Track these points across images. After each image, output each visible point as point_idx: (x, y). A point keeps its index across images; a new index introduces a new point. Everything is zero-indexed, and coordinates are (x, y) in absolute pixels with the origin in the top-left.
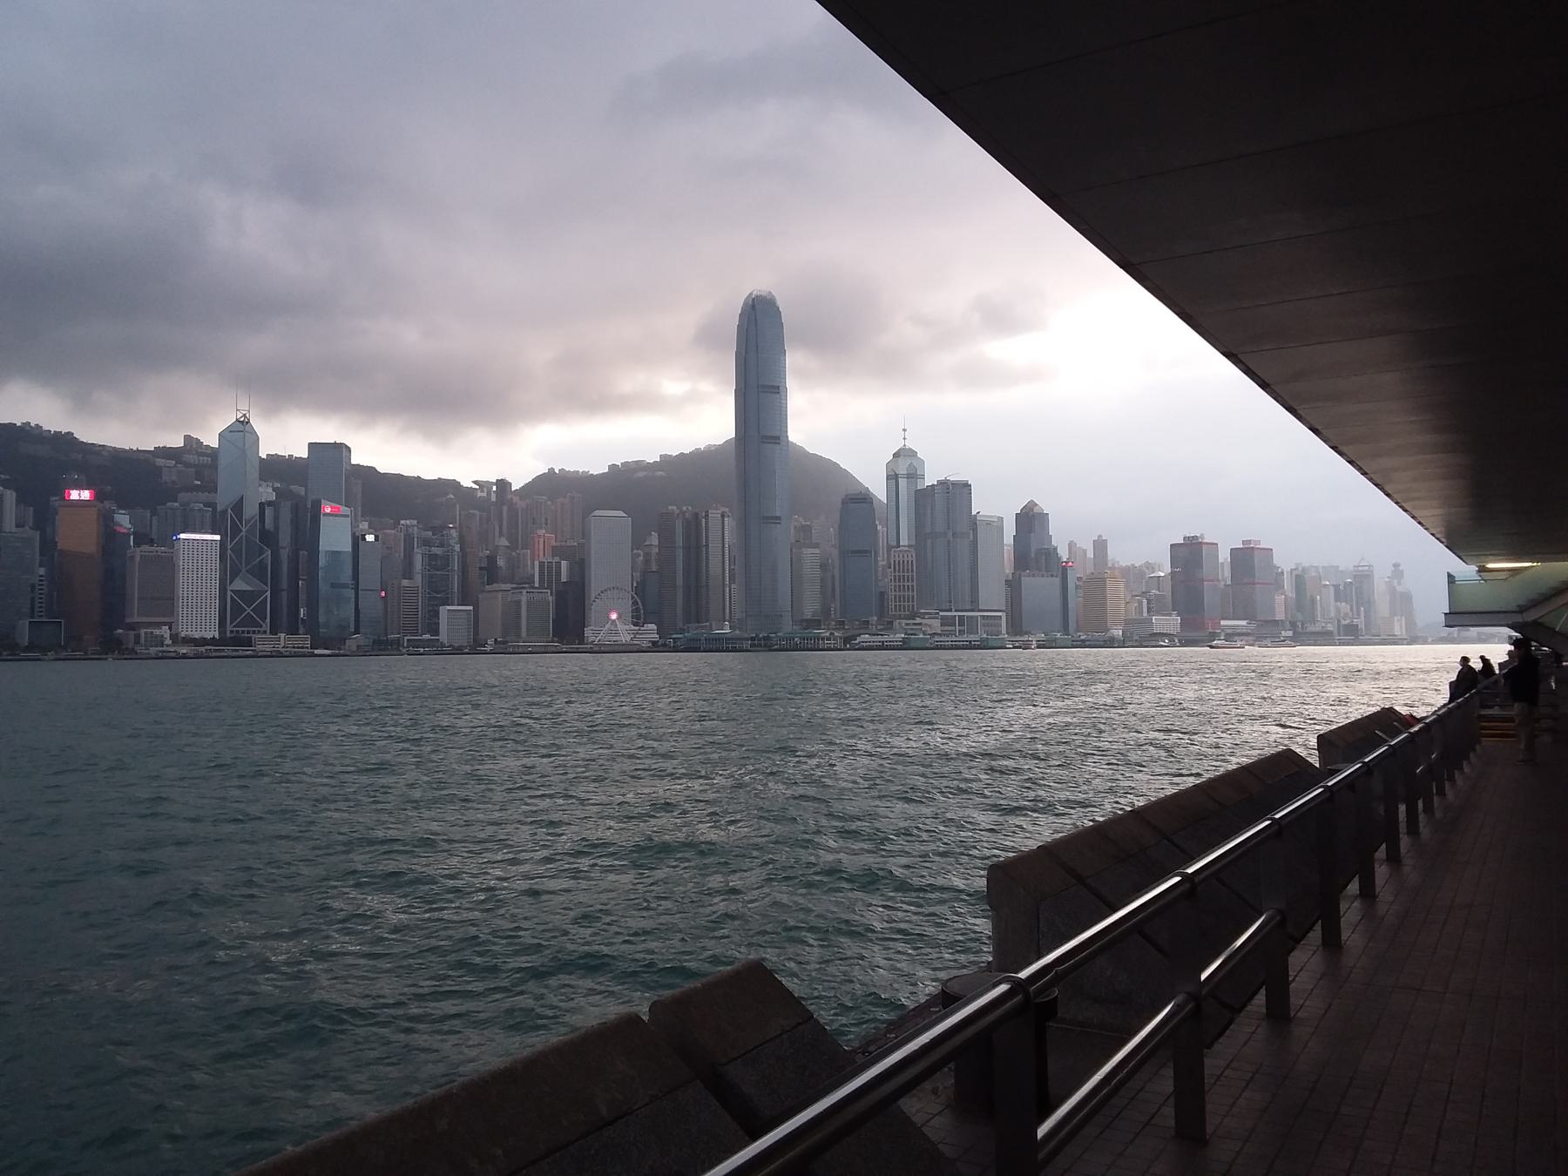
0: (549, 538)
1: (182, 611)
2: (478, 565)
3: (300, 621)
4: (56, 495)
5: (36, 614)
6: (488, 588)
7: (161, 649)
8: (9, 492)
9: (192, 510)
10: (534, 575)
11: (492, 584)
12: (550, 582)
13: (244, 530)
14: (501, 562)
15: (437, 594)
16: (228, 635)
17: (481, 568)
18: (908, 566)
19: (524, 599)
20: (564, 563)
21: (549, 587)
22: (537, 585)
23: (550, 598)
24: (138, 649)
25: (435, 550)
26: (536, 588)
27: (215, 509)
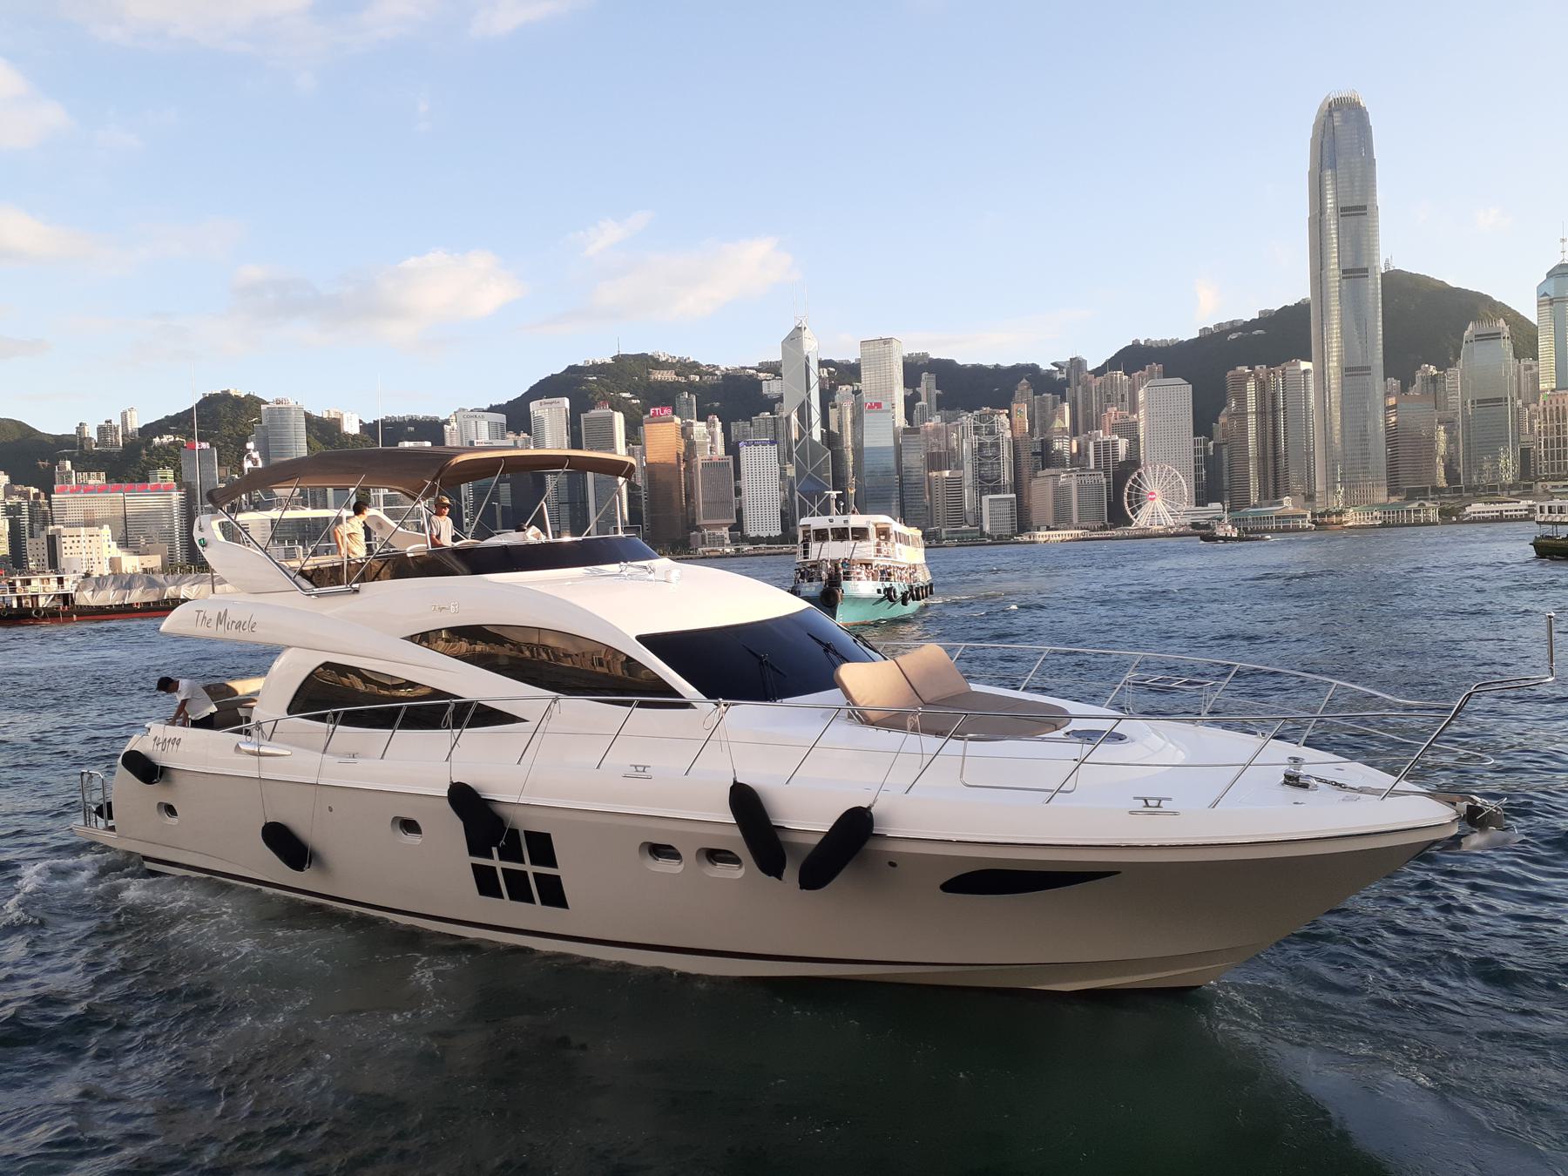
6: (1040, 473)
13: (807, 433)
15: (987, 484)
17: (1034, 454)
18: (1558, 413)
19: (1074, 483)
20: (1123, 445)
23: (1104, 481)
25: (989, 440)
26: (1091, 470)
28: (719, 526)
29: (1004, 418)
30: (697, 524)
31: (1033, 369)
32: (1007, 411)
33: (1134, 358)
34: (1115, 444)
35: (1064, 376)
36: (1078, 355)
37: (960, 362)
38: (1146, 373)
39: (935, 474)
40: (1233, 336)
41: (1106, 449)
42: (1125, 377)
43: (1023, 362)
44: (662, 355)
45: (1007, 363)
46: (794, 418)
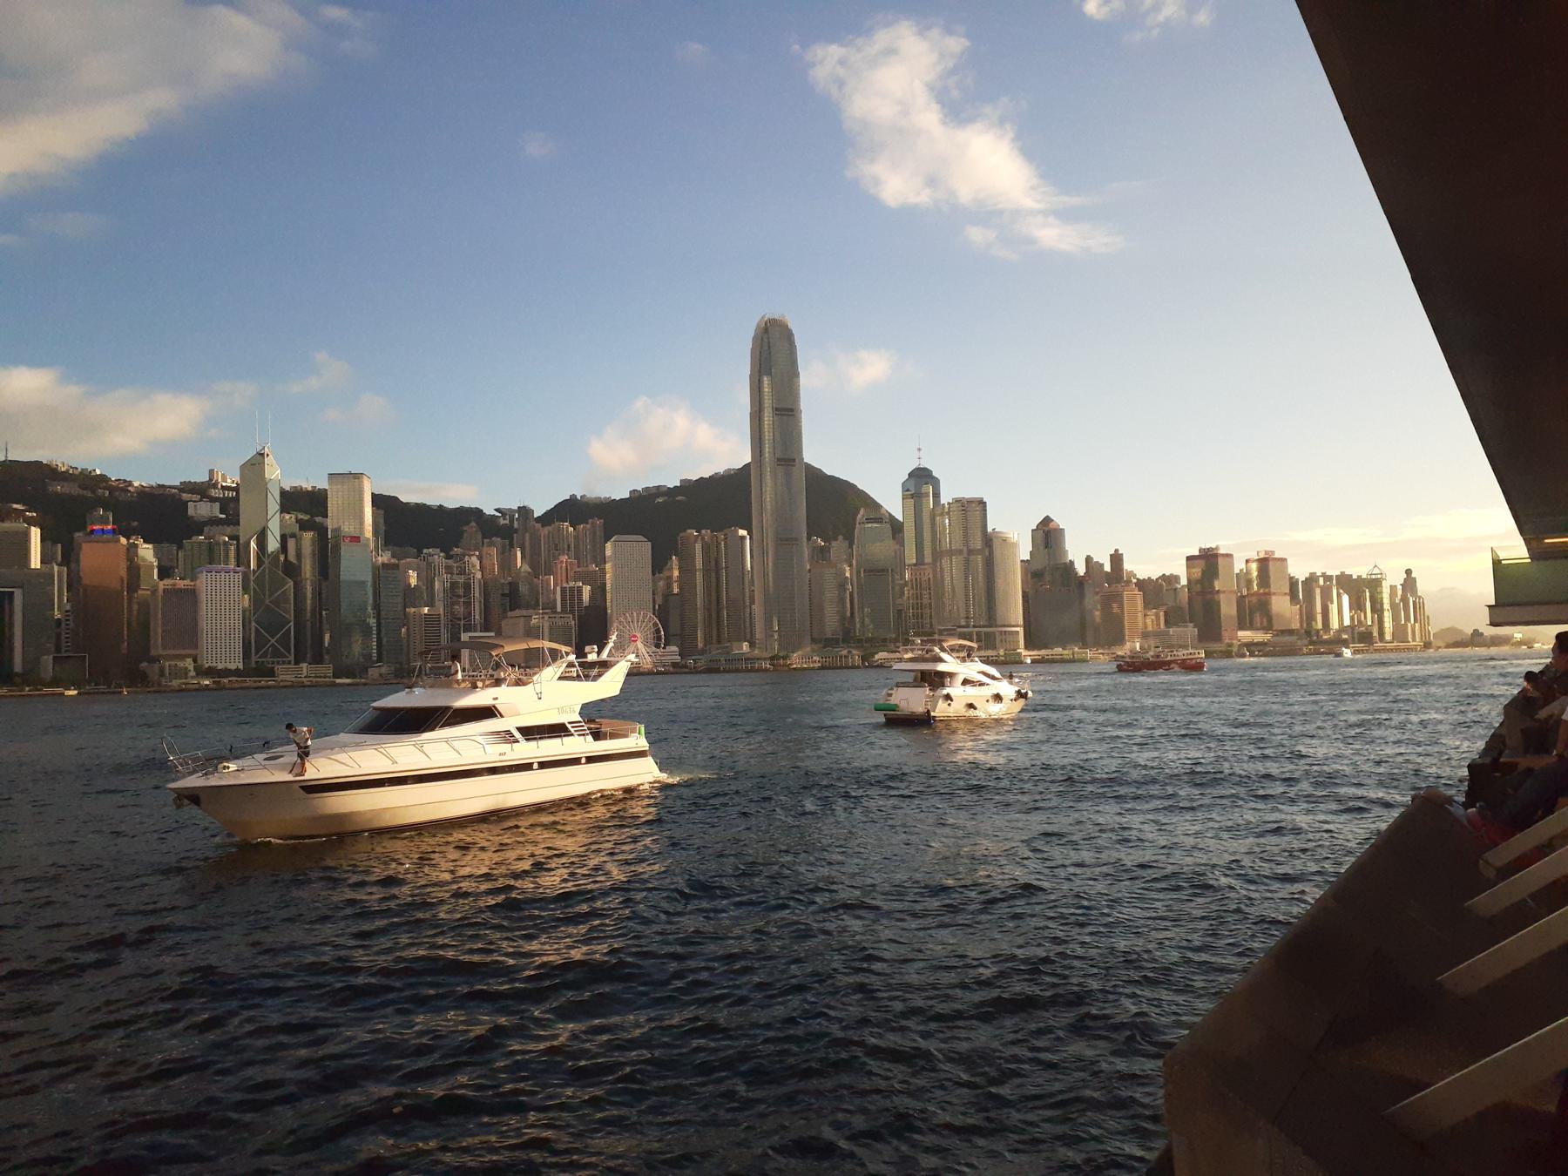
0: (572, 564)
1: (204, 642)
2: (500, 592)
3: (324, 651)
4: (79, 531)
5: (63, 650)
6: (510, 614)
7: (184, 681)
8: (33, 528)
9: (219, 544)
10: (555, 600)
11: (514, 610)
12: (572, 606)
14: (523, 589)
16: (253, 665)
17: (503, 595)
20: (586, 590)
21: (572, 612)
22: (559, 610)
24: (163, 681)
27: (238, 541)
28: (182, 657)
29: (474, 559)
30: (153, 652)
31: (477, 513)
32: (477, 553)
33: (571, 510)
34: (580, 590)
35: (507, 522)
36: (526, 504)
37: (404, 499)
38: (588, 526)
39: (413, 610)
40: (660, 500)
41: (571, 596)
42: (571, 529)
43: (466, 505)
44: (60, 465)
45: (451, 504)
46: (253, 544)
